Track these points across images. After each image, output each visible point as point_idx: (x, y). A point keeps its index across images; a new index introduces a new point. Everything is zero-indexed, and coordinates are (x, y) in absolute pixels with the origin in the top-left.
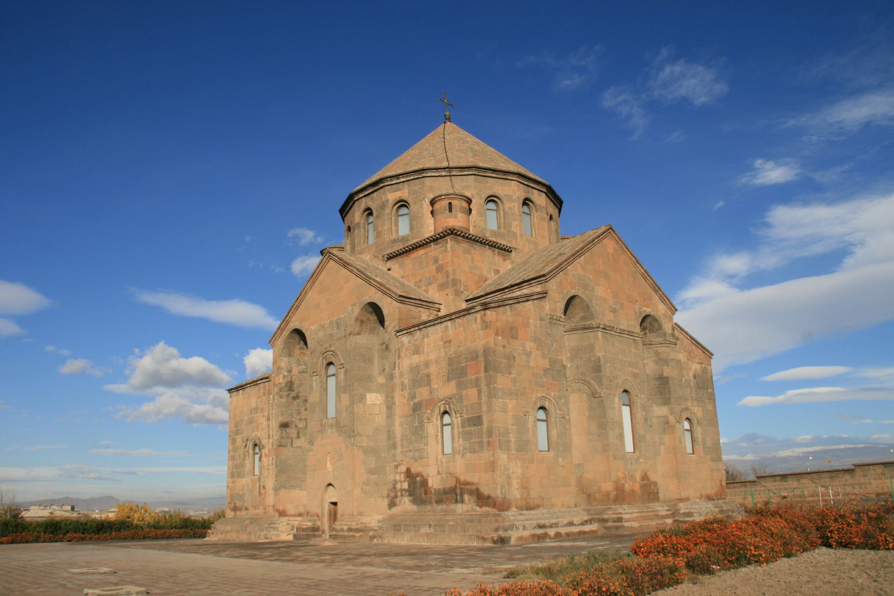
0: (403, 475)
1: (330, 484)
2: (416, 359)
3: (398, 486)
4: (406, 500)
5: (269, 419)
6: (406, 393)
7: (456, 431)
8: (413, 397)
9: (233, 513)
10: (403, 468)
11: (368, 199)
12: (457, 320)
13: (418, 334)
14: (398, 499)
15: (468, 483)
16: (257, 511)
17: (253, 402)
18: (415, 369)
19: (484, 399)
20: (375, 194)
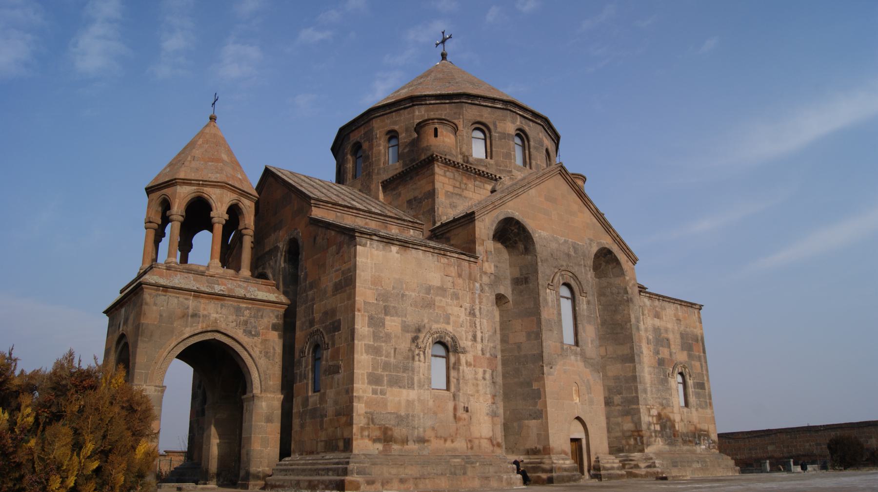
0: (655, 419)
1: (578, 418)
2: (657, 322)
3: (652, 427)
4: (659, 439)
5: (472, 314)
6: (652, 347)
7: (691, 390)
8: (658, 353)
9: (380, 446)
10: (654, 412)
11: (524, 121)
12: (684, 308)
13: (657, 303)
14: (653, 439)
15: (701, 430)
16: (449, 444)
17: (435, 278)
18: (657, 330)
19: (704, 372)
20: (531, 123)
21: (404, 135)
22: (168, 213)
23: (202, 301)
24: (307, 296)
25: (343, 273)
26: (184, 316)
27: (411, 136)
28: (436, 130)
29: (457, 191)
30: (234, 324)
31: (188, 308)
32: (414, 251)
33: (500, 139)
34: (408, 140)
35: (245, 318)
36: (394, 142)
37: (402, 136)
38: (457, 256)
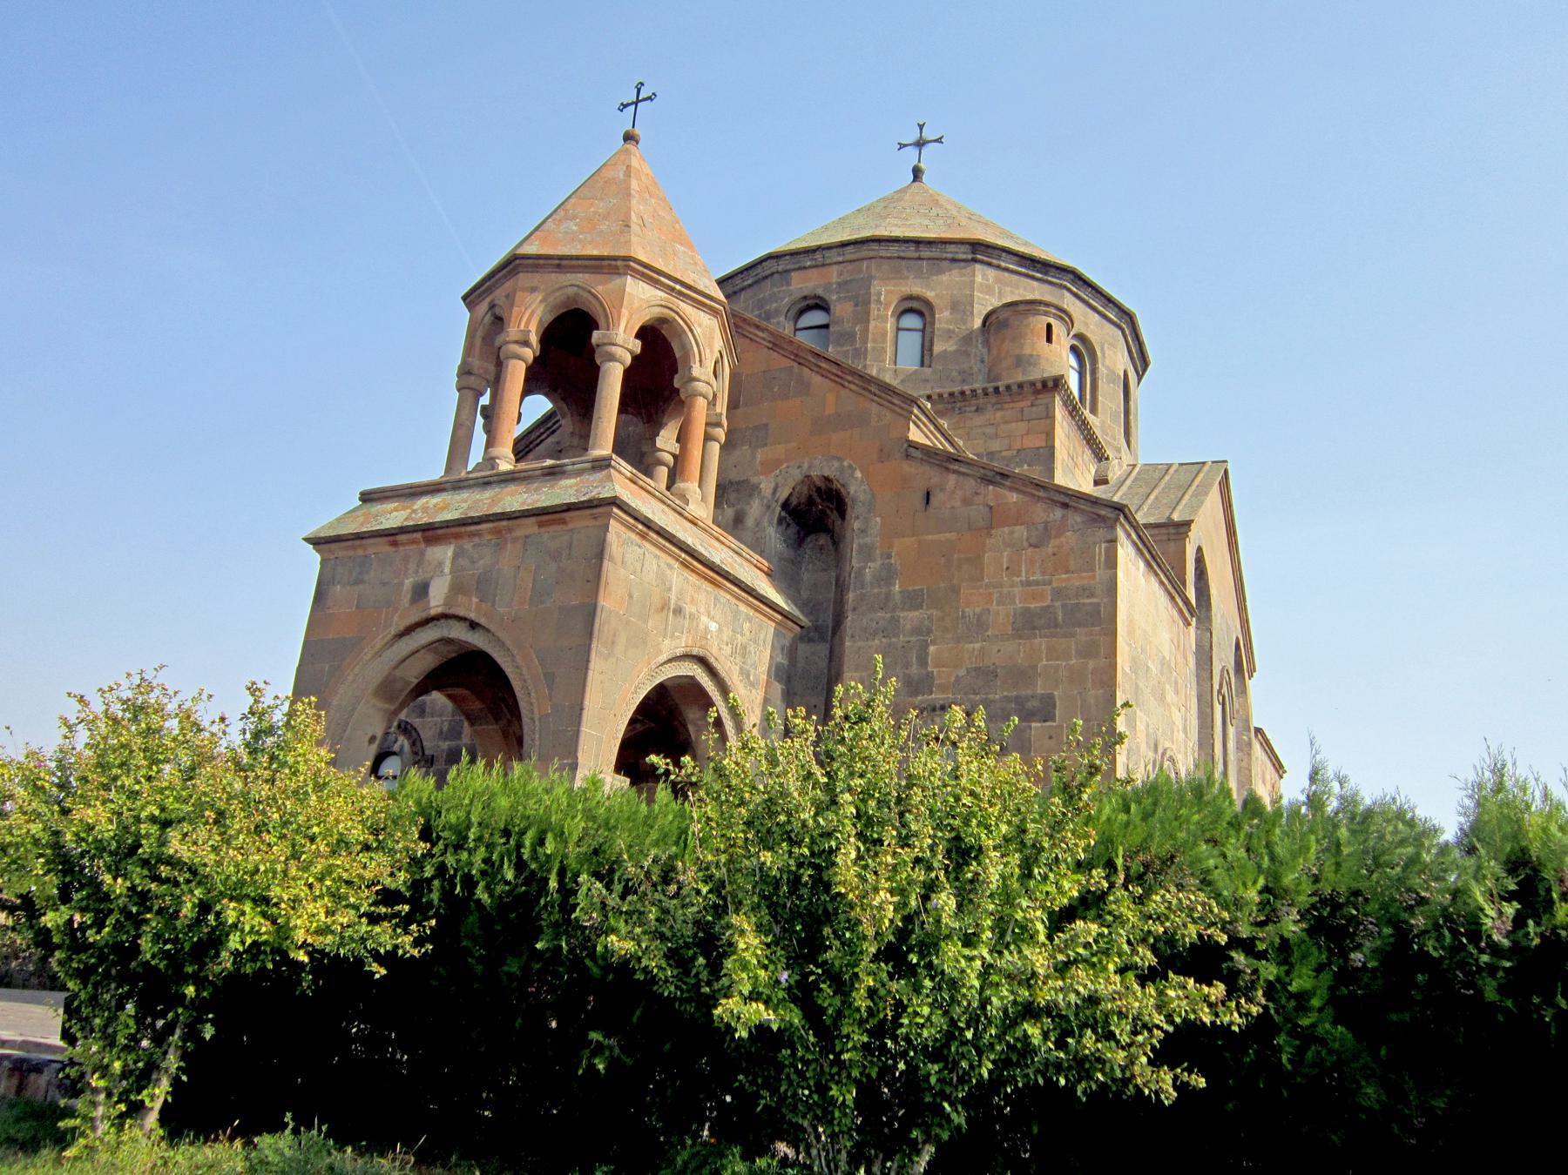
5: (1185, 730)
21: (946, 314)
22: (596, 336)
23: (693, 578)
24: (895, 620)
25: (1058, 593)
26: (664, 607)
27: (964, 322)
28: (1049, 326)
29: (1071, 464)
30: (727, 650)
31: (670, 589)
32: (1153, 579)
33: (1109, 382)
34: (962, 330)
35: (744, 640)
36: (911, 321)
37: (943, 317)
38: (1181, 603)
